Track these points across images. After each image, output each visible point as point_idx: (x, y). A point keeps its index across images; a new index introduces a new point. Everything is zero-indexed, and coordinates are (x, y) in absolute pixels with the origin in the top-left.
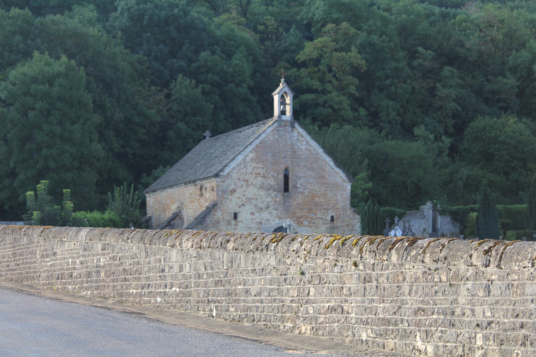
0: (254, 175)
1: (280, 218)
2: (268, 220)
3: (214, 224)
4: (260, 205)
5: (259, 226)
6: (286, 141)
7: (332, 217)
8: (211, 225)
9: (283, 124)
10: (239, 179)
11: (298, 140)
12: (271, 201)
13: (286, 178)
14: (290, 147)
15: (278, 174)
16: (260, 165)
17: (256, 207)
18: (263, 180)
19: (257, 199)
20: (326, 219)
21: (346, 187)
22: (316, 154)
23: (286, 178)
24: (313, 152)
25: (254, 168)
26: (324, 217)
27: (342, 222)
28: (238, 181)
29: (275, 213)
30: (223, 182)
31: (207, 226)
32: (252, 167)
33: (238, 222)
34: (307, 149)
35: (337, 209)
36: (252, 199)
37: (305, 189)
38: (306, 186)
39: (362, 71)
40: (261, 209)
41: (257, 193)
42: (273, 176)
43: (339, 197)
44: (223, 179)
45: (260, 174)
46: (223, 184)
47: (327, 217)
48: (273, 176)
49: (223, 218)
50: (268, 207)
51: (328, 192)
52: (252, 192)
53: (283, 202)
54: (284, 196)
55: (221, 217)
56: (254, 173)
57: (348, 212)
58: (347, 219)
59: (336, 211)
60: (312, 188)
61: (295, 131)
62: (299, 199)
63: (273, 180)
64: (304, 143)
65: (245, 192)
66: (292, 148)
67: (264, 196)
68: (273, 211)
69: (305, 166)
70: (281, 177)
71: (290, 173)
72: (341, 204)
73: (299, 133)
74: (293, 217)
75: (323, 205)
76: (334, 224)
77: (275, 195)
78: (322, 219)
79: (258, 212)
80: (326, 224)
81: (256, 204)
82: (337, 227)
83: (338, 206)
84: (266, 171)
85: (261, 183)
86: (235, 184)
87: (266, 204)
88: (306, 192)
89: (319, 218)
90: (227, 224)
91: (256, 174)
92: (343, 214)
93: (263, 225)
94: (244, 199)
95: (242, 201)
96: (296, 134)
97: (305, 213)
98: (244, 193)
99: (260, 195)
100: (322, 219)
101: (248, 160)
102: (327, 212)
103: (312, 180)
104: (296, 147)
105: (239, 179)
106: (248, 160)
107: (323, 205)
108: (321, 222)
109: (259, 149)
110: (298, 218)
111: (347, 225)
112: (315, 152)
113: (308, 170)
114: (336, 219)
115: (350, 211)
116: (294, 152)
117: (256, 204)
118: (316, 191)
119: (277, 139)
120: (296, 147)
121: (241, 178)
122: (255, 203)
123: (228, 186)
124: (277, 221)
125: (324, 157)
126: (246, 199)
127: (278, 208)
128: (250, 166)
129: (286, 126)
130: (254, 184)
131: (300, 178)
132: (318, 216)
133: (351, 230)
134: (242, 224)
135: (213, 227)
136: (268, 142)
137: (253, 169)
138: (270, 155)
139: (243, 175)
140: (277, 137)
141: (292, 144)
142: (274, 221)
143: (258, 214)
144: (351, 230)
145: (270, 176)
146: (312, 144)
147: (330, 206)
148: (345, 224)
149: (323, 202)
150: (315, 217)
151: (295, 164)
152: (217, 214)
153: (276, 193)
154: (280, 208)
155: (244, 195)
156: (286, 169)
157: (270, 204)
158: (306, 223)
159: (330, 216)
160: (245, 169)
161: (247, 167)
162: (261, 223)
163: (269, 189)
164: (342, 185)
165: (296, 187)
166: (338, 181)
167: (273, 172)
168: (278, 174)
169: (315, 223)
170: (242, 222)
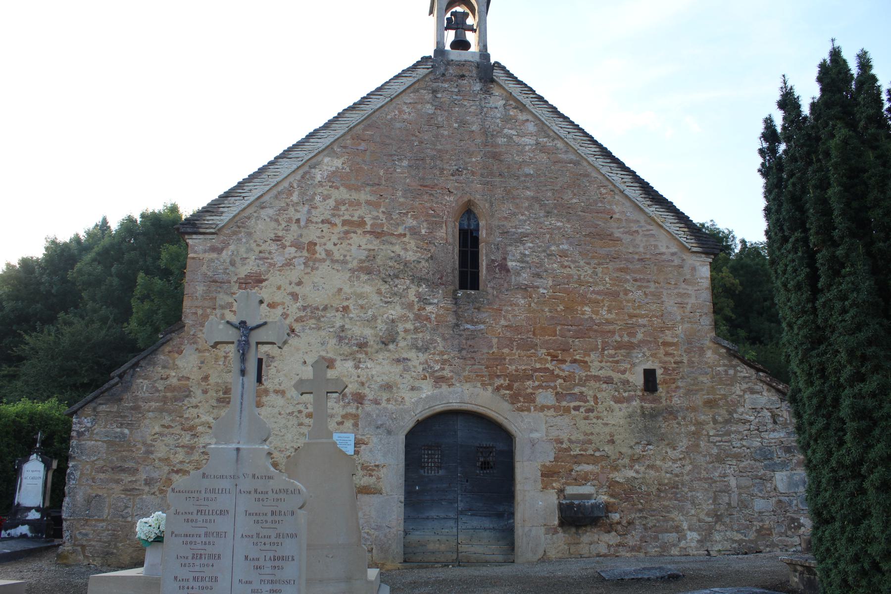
0: (340, 228)
1: (439, 380)
2: (388, 387)
3: (165, 400)
4: (358, 331)
5: (351, 410)
6: (463, 123)
7: (649, 375)
8: (153, 404)
9: (451, 70)
10: (277, 239)
11: (507, 119)
12: (404, 318)
13: (469, 241)
14: (478, 141)
15: (434, 225)
16: (363, 196)
17: (341, 339)
18: (375, 244)
19: (346, 309)
20: (626, 382)
21: (694, 269)
22: (576, 163)
23: (469, 241)
24: (563, 156)
25: (339, 203)
26: (616, 376)
27: (689, 392)
28: (274, 247)
29: (417, 359)
30: (213, 249)
31: (136, 408)
32: (331, 202)
33: (266, 392)
34: (540, 147)
35: (665, 344)
36: (325, 309)
37: (538, 275)
38: (541, 265)
39: (737, 292)
40: (362, 346)
41: (347, 289)
42: (414, 231)
43: (670, 304)
44: (215, 241)
45: (362, 223)
46: (215, 255)
47: (627, 376)
48: (414, 231)
49: (206, 378)
50: (388, 340)
51: (628, 286)
52: (326, 284)
53: (451, 319)
54: (456, 299)
55: (196, 375)
56: (338, 221)
57: (709, 354)
58: (705, 379)
59: (662, 351)
60: (566, 271)
61: (496, 91)
62: (518, 310)
63: (412, 244)
64: (531, 127)
65: (299, 283)
66: (485, 145)
67: (375, 298)
68: (412, 354)
69: (536, 199)
70: (447, 235)
71: (482, 223)
72: (680, 330)
74: (493, 376)
75: (613, 333)
76: (657, 400)
77: (419, 295)
78: (609, 381)
79: (351, 356)
80: (628, 400)
81: (343, 329)
82: (671, 413)
83: (668, 337)
84: (388, 215)
85: (363, 255)
86: (263, 257)
87: (381, 326)
88: (545, 285)
89: (597, 378)
90: (219, 400)
91: (345, 223)
92: (691, 363)
93: (368, 407)
94: (294, 309)
95: (285, 316)
97: (540, 360)
98: (297, 289)
99: (361, 296)
100: (609, 381)
101: (318, 178)
102: (628, 355)
103: (565, 247)
104: (501, 141)
105: (277, 239)
106: (318, 178)
107: (613, 333)
108: (606, 393)
110: (513, 378)
111: (711, 404)
112: (573, 157)
113: (548, 214)
114: (665, 382)
115: (715, 352)
116: (496, 156)
117: (343, 329)
118: (580, 283)
119: (431, 117)
120: (501, 141)
121: (289, 238)
122: (338, 324)
123: (233, 263)
124: (427, 389)
125: (604, 170)
126: (304, 308)
127: (433, 341)
128: (326, 198)
129: (462, 77)
130: (337, 256)
131: (520, 240)
132: (594, 372)
133: (727, 422)
134: (279, 401)
135: (161, 410)
136: (398, 125)
137: (336, 208)
138: (405, 163)
139: (294, 227)
140: (429, 109)
141: (485, 132)
142: (413, 389)
143: (350, 364)
144: (727, 422)
145: (401, 230)
146: (555, 128)
147: (640, 336)
148: (699, 399)
149: (608, 322)
150: (581, 373)
151: (499, 192)
152: (180, 363)
153: (423, 289)
154: (440, 345)
155: (295, 296)
156: (468, 212)
157: (400, 328)
158: (546, 397)
159: (640, 370)
160: (306, 208)
161: (312, 199)
162: (359, 399)
163: (397, 277)
164: (677, 262)
165: (504, 268)
166: (663, 250)
167: (415, 217)
168: (434, 225)
169: (582, 397)
170: (281, 393)
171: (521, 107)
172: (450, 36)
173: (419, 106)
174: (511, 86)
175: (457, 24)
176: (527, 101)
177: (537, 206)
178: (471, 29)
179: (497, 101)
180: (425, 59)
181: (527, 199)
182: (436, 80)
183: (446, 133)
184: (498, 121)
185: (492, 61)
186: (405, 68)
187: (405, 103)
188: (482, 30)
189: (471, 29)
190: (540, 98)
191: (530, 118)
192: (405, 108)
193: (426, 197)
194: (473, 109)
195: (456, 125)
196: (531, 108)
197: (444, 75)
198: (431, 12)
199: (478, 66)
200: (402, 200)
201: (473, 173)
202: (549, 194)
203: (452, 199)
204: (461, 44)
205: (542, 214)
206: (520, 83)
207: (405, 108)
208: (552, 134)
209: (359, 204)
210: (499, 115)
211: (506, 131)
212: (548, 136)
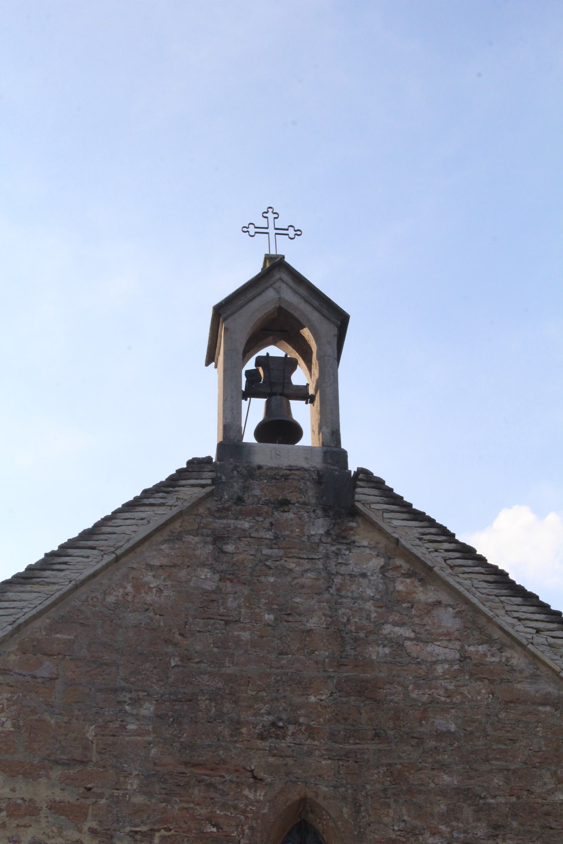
6: (286, 612)
11: (389, 602)
14: (323, 654)
16: (44, 792)
24: (525, 687)
61: (363, 537)
64: (447, 619)
69: (465, 793)
73: (395, 547)
96: (377, 563)
109: (47, 668)
116: (366, 690)
120: (377, 652)
129: (284, 504)
136: (132, 618)
138: (148, 709)
140: (206, 579)
141: (338, 632)
146: (505, 621)
171: (423, 573)
172: (254, 411)
173: (183, 574)
174: (397, 525)
175: (273, 384)
176: (435, 560)
177: (468, 812)
178: (302, 394)
179: (364, 559)
180: (196, 465)
181: (443, 793)
182: (222, 512)
183: (245, 636)
184: (369, 606)
185: (352, 467)
186: (150, 485)
187: (150, 567)
188: (326, 397)
189: (302, 394)
190: (468, 552)
191: (444, 598)
192: (149, 577)
193: (197, 792)
194: (308, 579)
195: (269, 617)
196: (446, 574)
197: (240, 500)
198: (211, 358)
199: (320, 479)
200: (138, 799)
201: (311, 732)
202: (498, 781)
203: (260, 795)
204: (278, 429)
205: (481, 830)
206: (419, 516)
207: (149, 577)
208: (497, 634)
209: (32, 810)
210: (370, 592)
211: (387, 629)
212: (489, 640)
